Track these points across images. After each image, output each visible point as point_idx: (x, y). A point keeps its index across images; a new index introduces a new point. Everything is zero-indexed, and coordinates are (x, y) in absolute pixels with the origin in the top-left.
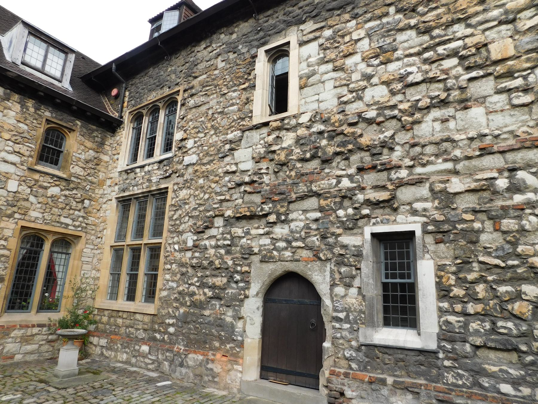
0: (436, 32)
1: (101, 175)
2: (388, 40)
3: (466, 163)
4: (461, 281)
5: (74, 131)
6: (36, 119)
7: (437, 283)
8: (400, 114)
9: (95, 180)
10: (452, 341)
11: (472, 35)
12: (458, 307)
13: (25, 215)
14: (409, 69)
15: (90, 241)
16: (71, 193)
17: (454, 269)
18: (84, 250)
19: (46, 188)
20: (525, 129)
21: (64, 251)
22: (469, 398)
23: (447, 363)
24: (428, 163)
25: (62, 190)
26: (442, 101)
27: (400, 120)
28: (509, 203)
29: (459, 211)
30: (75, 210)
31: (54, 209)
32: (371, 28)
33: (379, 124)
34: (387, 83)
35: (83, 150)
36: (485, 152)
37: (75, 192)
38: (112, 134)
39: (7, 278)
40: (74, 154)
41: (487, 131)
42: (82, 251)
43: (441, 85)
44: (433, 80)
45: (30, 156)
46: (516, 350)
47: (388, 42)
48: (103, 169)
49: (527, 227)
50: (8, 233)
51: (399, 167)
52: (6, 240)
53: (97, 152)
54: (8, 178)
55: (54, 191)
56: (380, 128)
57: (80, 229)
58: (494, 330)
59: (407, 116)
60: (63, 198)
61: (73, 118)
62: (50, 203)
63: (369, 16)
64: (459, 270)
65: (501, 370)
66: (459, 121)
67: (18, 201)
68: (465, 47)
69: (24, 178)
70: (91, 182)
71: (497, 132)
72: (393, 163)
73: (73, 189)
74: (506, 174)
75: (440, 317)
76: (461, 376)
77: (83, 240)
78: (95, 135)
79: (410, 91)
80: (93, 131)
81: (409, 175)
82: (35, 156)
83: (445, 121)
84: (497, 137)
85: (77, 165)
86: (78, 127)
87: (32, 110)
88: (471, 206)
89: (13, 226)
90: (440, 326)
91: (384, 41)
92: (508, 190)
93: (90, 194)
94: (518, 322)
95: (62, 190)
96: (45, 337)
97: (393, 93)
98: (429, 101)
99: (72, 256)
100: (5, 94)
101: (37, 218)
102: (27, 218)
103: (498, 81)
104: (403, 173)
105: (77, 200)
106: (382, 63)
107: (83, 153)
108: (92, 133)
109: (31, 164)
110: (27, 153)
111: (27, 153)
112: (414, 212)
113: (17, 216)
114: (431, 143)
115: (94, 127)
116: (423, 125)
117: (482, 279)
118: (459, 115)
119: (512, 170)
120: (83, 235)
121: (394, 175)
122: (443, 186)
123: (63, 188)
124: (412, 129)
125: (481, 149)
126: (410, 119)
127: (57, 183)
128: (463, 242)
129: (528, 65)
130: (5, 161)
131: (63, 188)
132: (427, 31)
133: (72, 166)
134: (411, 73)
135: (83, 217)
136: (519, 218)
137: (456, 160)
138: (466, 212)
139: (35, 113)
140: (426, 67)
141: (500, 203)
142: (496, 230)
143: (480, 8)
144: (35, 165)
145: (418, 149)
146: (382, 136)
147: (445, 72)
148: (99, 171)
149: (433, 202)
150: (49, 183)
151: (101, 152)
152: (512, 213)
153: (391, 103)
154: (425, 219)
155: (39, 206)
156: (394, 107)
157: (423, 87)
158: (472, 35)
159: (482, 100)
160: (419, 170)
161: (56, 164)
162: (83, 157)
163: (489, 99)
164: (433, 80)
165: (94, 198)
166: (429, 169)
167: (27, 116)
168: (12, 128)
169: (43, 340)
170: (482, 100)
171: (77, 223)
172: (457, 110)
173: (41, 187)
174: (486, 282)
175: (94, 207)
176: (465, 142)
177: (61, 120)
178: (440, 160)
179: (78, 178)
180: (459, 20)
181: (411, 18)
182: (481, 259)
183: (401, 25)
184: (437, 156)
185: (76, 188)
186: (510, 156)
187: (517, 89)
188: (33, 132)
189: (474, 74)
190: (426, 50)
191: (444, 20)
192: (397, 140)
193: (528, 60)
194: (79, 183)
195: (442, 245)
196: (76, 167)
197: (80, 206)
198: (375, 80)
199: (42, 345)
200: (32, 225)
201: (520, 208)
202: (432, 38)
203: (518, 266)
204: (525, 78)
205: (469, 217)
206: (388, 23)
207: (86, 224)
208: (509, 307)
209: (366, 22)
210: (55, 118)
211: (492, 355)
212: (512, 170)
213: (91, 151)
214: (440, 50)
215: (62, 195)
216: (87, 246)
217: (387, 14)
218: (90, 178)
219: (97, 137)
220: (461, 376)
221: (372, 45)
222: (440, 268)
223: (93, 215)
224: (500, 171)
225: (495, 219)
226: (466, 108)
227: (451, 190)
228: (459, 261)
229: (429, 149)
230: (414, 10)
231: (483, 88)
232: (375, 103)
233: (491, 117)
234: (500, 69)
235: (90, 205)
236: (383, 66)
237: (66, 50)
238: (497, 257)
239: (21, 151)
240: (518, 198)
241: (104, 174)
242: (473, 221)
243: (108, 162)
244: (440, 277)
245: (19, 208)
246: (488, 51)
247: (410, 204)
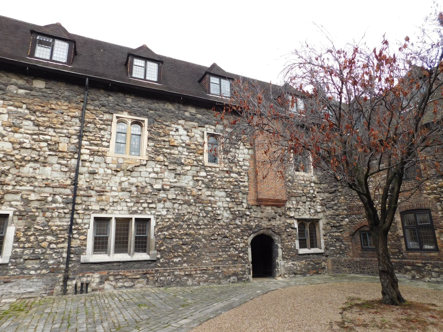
0: (41, 128)
2: (19, 121)
3: (39, 188)
4: (25, 235)
7: (15, 236)
8: (15, 160)
10: (15, 258)
11: (55, 136)
12: (21, 245)
14: (25, 140)
17: (23, 230)
20: (62, 180)
22: (17, 278)
23: (12, 267)
24: (23, 185)
26: (36, 160)
27: (14, 163)
28: (50, 207)
29: (31, 208)
32: (11, 111)
33: (3, 161)
34: (12, 143)
36: (47, 186)
41: (49, 178)
43: (37, 153)
44: (34, 149)
46: (39, 259)
47: (18, 122)
49: (54, 216)
51: (9, 185)
56: (3, 163)
58: (33, 253)
59: (19, 162)
63: (11, 103)
64: (26, 231)
65: (32, 267)
66: (40, 171)
68: (51, 140)
71: (53, 179)
72: (6, 182)
74: (52, 196)
75: (13, 249)
76: (16, 271)
79: (22, 150)
81: (13, 189)
83: (35, 169)
84: (53, 181)
88: (36, 206)
90: (12, 253)
91: (16, 121)
92: (51, 202)
94: (43, 249)
97: (14, 149)
98: (30, 158)
103: (59, 159)
104: (10, 188)
106: (12, 131)
112: (11, 206)
114: (26, 177)
116: (25, 168)
117: (33, 234)
118: (41, 168)
119: (55, 195)
121: (5, 188)
122: (27, 196)
124: (19, 168)
125: (46, 185)
126: (19, 164)
128: (29, 220)
129: (70, 157)
132: (38, 125)
134: (24, 142)
136: (52, 212)
137: (35, 187)
138: (34, 208)
140: (33, 142)
141: (47, 206)
142: (43, 216)
143: (60, 126)
145: (20, 178)
146: (3, 168)
147: (41, 148)
149: (21, 202)
152: (50, 210)
153: (12, 153)
154: (15, 209)
156: (13, 156)
157: (30, 150)
158: (55, 136)
159: (51, 165)
160: (18, 187)
163: (54, 165)
164: (34, 149)
166: (23, 188)
170: (51, 165)
172: (41, 166)
174: (35, 235)
176: (41, 180)
178: (29, 185)
180: (52, 127)
181: (32, 115)
182: (35, 227)
183: (27, 117)
184: (28, 183)
186: (55, 189)
187: (64, 165)
189: (51, 153)
190: (35, 134)
191: (46, 124)
192: (10, 171)
193: (70, 155)
195: (21, 221)
198: (6, 139)
201: (53, 209)
202: (39, 130)
203: (47, 230)
204: (68, 161)
205: (34, 210)
206: (20, 113)
208: (41, 244)
209: (9, 105)
211: (31, 262)
212: (55, 195)
214: (41, 137)
217: (21, 107)
220: (16, 271)
221: (9, 120)
222: (18, 230)
224: (50, 194)
225: (44, 212)
226: (44, 166)
227: (30, 199)
228: (26, 227)
229: (25, 179)
230: (35, 112)
231: (53, 160)
232: (3, 151)
233: (53, 172)
234: (60, 154)
236: (12, 133)
238: (41, 226)
240: (54, 205)
242: (36, 212)
244: (17, 234)
246: (59, 145)
247: (10, 202)
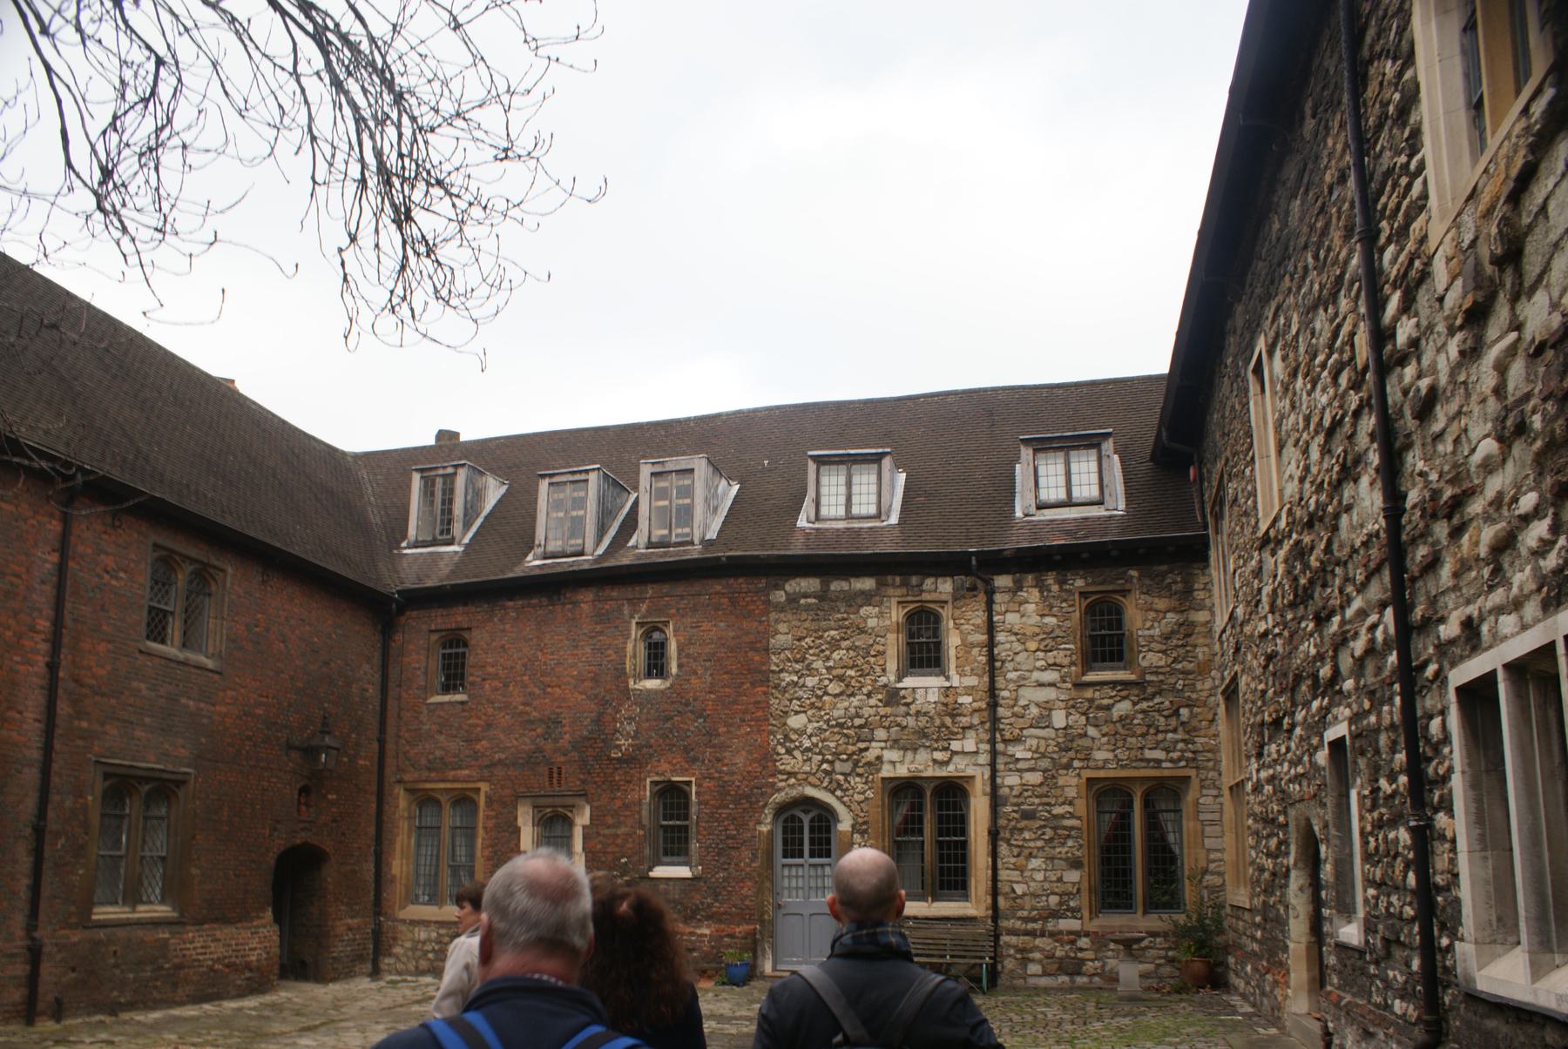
1: (1201, 653)
5: (1129, 591)
6: (1065, 601)
9: (1190, 666)
13: (1088, 759)
15: (1207, 782)
16: (1151, 704)
18: (1201, 801)
19: (1108, 708)
21: (1172, 807)
25: (1135, 704)
30: (1166, 732)
31: (1129, 739)
35: (1154, 620)
37: (1158, 700)
38: (1201, 566)
39: (1085, 862)
40: (1140, 633)
42: (1197, 803)
45: (1072, 664)
48: (1201, 641)
50: (1071, 793)
52: (1071, 804)
53: (1182, 612)
54: (1051, 710)
55: (1123, 708)
57: (1183, 763)
60: (1140, 716)
61: (1121, 570)
62: (1121, 731)
67: (1072, 741)
69: (1071, 703)
70: (1183, 673)
73: (1153, 696)
77: (1195, 783)
78: (1169, 581)
80: (1163, 575)
82: (1079, 662)
85: (1150, 650)
86: (1135, 581)
87: (1055, 588)
89: (1074, 781)
93: (1187, 694)
95: (1135, 704)
96: (1162, 953)
99: (1184, 810)
100: (1014, 582)
101: (1106, 761)
102: (1092, 764)
105: (1166, 713)
107: (1156, 624)
108: (1163, 581)
109: (1076, 676)
110: (1066, 661)
111: (1066, 661)
113: (1076, 764)
115: (1164, 568)
120: (1192, 773)
123: (1136, 699)
127: (1124, 693)
130: (1041, 685)
131: (1136, 699)
133: (1141, 655)
135: (1183, 741)
139: (1061, 590)
144: (1083, 675)
148: (1195, 646)
150: (1111, 697)
151: (1190, 608)
155: (1105, 740)
161: (1120, 658)
162: (1156, 632)
165: (1197, 700)
167: (1052, 601)
168: (1037, 630)
169: (1160, 958)
171: (1175, 755)
173: (1100, 708)
175: (1200, 717)
177: (1101, 584)
179: (1157, 673)
185: (1160, 693)
188: (1067, 624)
194: (1162, 681)
196: (1150, 655)
197: (1173, 722)
199: (1159, 965)
200: (1102, 774)
207: (1194, 752)
210: (1094, 583)
213: (1169, 615)
215: (1136, 712)
216: (1205, 792)
218: (1179, 666)
219: (1175, 582)
223: (1202, 733)
235: (1193, 716)
237: (1095, 441)
239: (1058, 661)
241: (1206, 649)
243: (1208, 622)
245: (1077, 751)
